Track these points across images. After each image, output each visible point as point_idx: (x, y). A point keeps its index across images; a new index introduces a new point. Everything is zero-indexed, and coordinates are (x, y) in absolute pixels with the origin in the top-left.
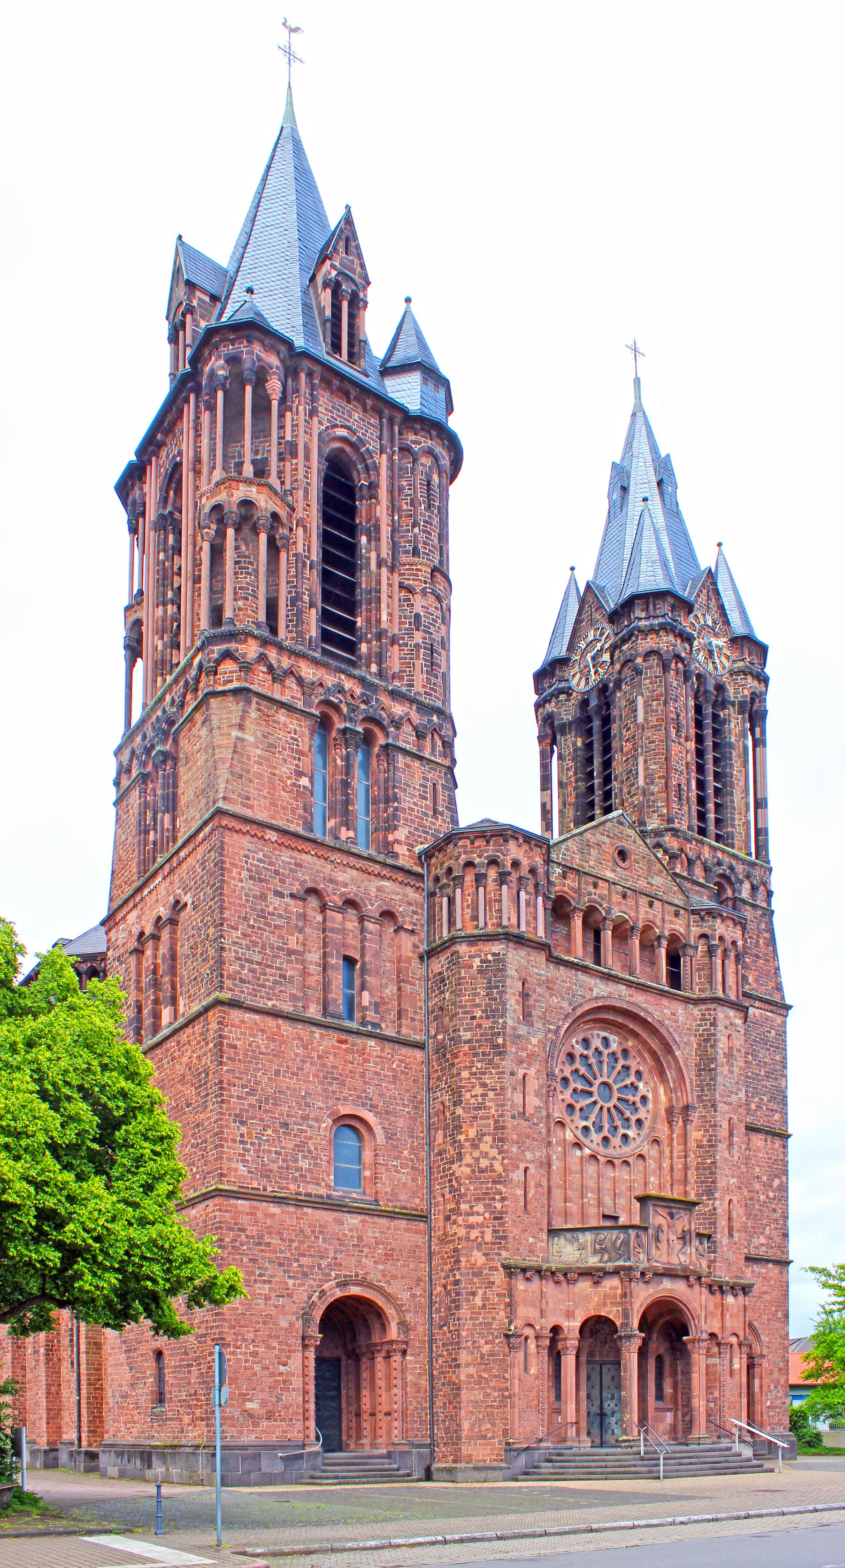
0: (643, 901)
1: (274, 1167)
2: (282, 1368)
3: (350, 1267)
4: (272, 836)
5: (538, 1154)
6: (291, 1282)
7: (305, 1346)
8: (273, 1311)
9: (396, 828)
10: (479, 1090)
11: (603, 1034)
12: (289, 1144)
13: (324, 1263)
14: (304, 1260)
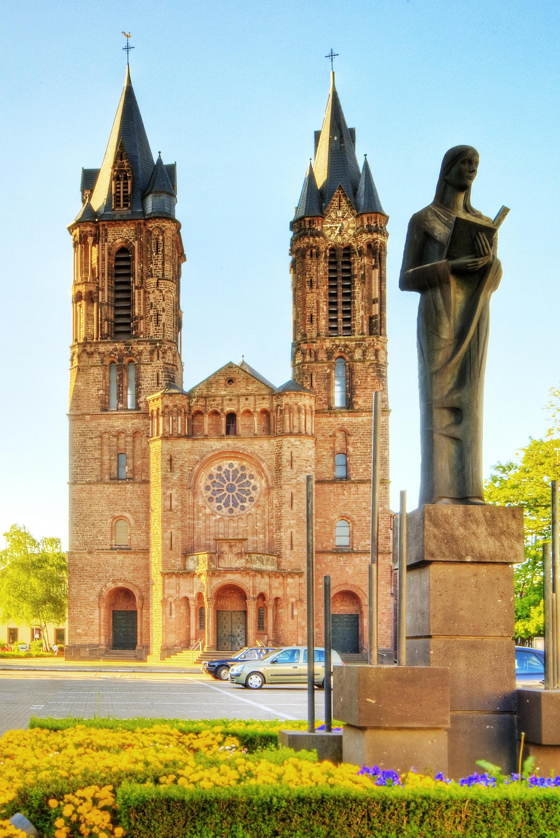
0: (242, 399)
1: (89, 540)
2: (91, 616)
3: (118, 575)
4: (88, 417)
5: (176, 525)
6: (94, 583)
7: (99, 607)
8: (87, 595)
9: (140, 397)
10: (154, 502)
11: (229, 462)
12: (95, 531)
13: (108, 575)
14: (100, 575)
